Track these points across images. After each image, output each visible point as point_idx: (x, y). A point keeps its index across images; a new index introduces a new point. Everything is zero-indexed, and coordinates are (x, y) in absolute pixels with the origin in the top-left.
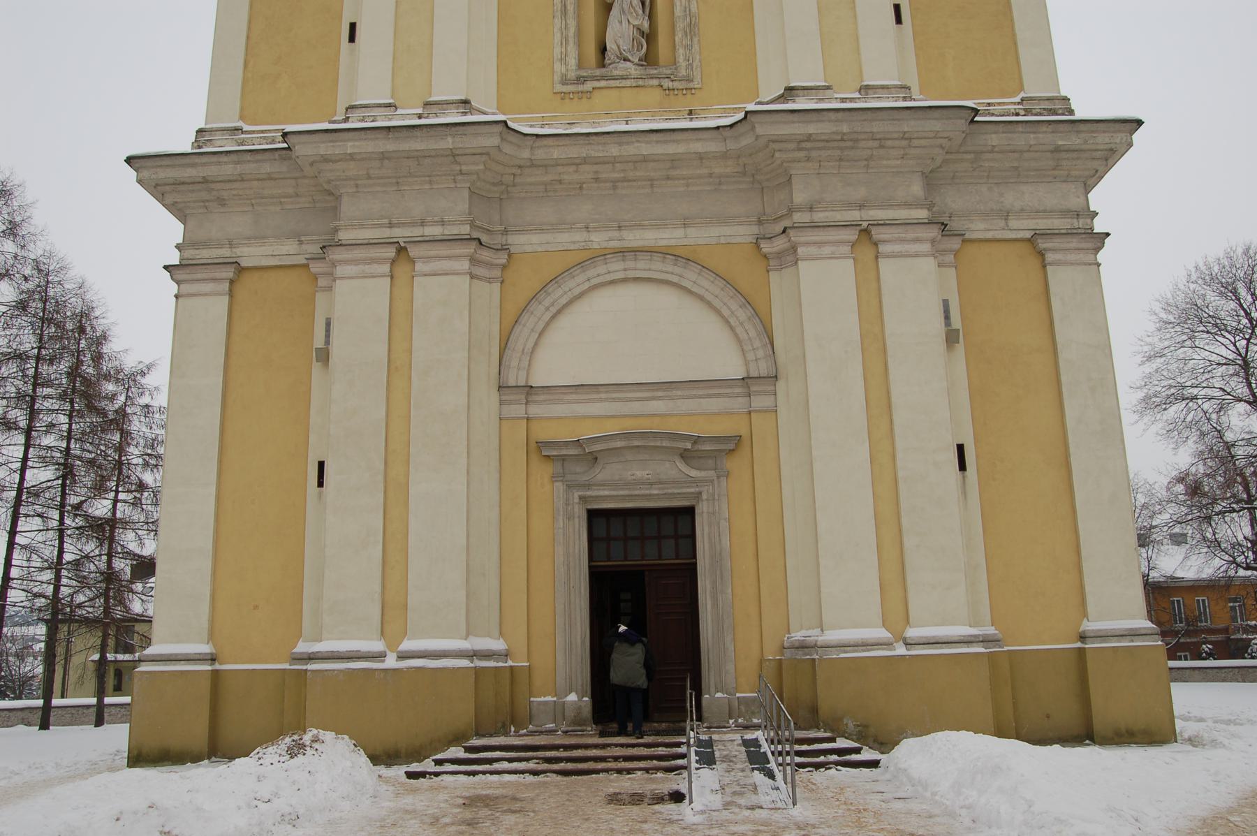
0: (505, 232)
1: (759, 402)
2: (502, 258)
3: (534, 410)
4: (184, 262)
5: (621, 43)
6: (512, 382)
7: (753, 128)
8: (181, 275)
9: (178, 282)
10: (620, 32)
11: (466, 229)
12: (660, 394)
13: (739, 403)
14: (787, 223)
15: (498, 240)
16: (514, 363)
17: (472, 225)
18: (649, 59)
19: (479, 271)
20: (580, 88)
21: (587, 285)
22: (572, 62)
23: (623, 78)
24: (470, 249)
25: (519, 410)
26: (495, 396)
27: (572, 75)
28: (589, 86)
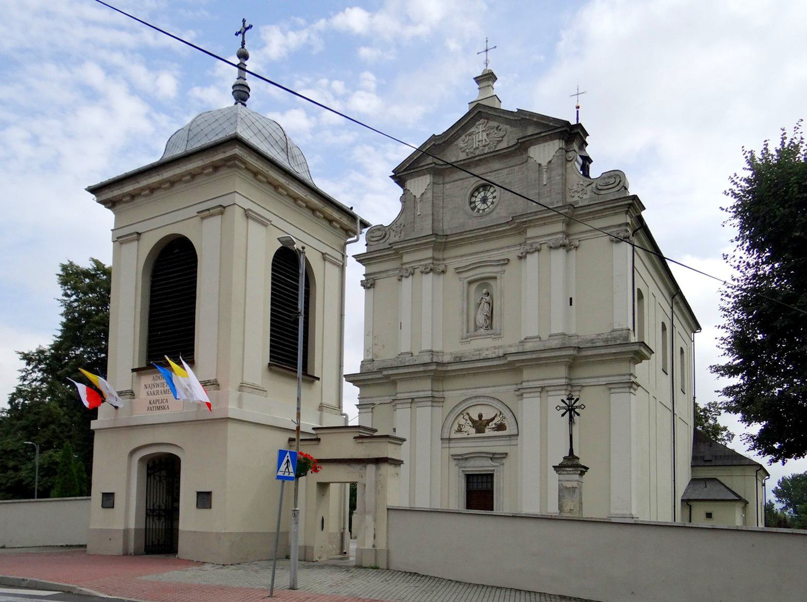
0: (443, 391)
1: (513, 442)
2: (442, 400)
3: (451, 445)
4: (361, 403)
5: (481, 322)
6: (445, 437)
7: (507, 359)
8: (360, 407)
9: (359, 409)
10: (481, 319)
11: (429, 393)
12: (486, 440)
13: (508, 443)
14: (519, 386)
15: (440, 394)
16: (446, 431)
17: (432, 391)
18: (490, 326)
19: (434, 404)
20: (467, 340)
21: (466, 407)
22: (465, 330)
23: (481, 335)
24: (431, 399)
25: (447, 445)
26: (440, 441)
27: (465, 336)
28: (469, 339)
